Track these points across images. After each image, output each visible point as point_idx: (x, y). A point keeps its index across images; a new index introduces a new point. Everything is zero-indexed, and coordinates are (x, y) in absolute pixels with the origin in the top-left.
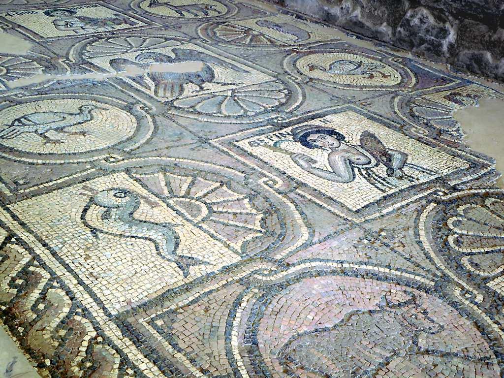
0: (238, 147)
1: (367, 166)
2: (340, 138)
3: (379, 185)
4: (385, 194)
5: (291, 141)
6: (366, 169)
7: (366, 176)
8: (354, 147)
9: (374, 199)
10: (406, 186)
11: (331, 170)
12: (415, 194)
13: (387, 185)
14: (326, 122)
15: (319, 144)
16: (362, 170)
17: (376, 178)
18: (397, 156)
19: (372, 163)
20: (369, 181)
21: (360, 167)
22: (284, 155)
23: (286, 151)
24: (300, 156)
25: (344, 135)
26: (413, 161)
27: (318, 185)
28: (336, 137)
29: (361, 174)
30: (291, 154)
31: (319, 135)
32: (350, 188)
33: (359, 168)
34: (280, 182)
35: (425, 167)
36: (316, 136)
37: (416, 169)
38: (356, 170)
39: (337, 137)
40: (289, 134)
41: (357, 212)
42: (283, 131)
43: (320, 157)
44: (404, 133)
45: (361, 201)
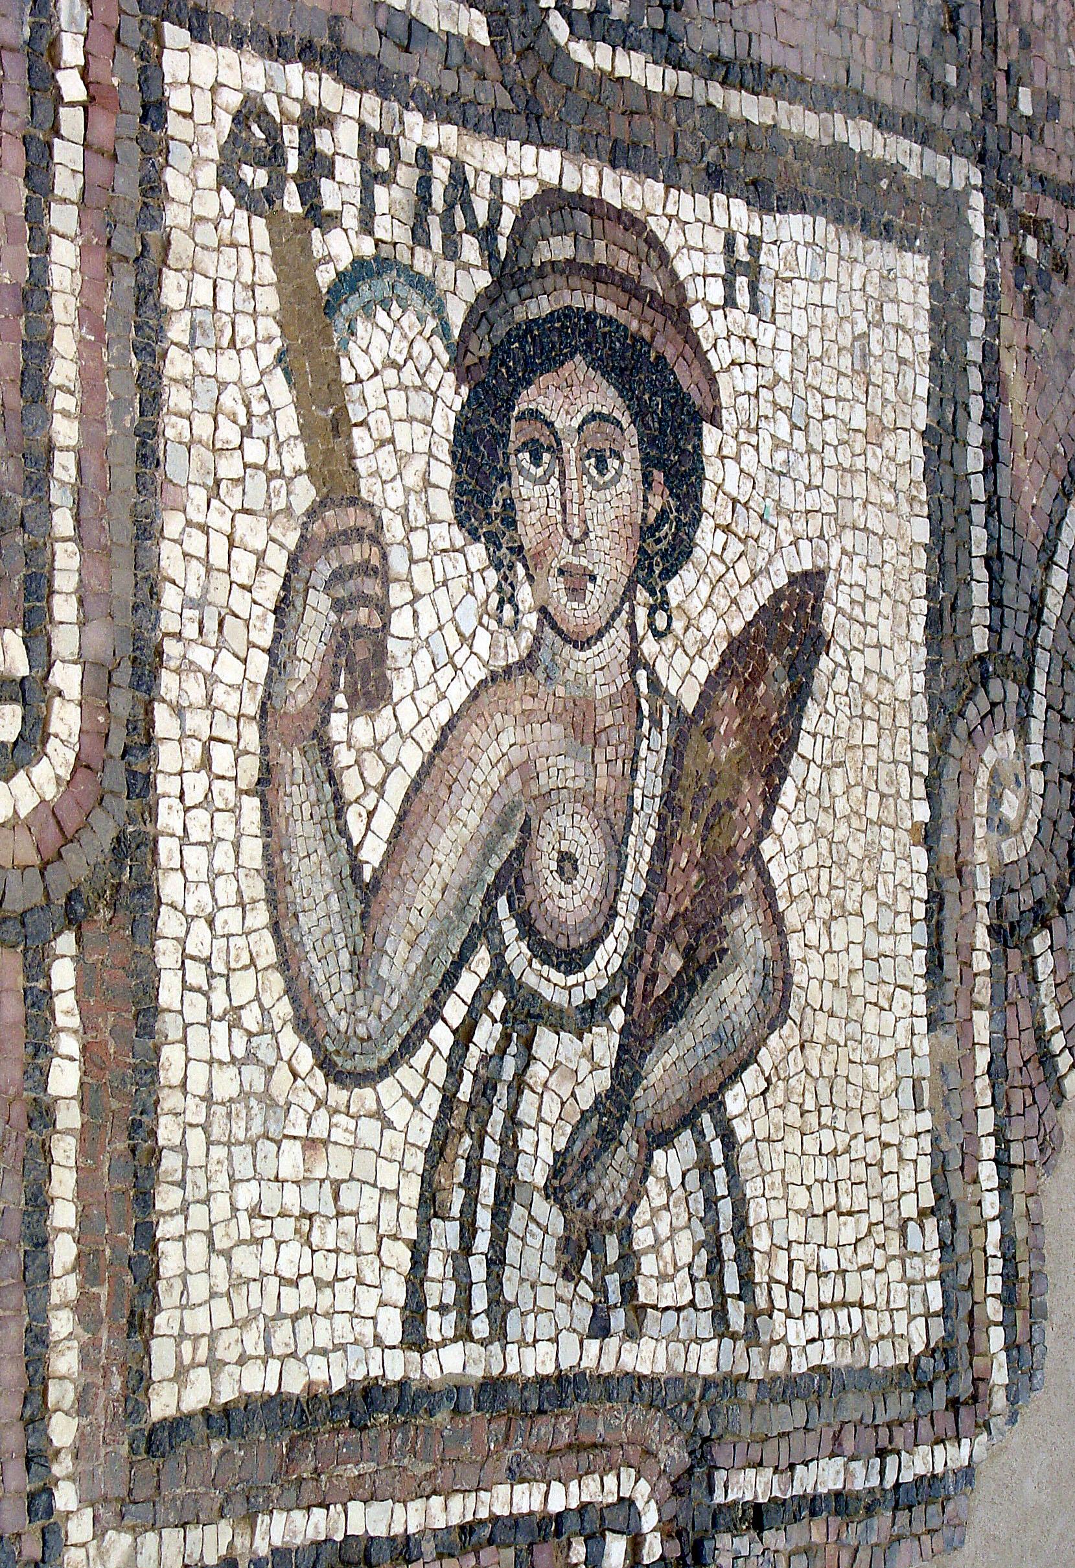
0: (154, 110)
1: (551, 985)
2: (661, 551)
3: (447, 1234)
4: (395, 1366)
5: (444, 329)
6: (527, 1016)
7: (465, 1092)
8: (641, 693)
9: (318, 1370)
10: (538, 1362)
11: (373, 853)
12: (516, 1476)
13: (478, 1269)
14: (742, 282)
15: (532, 493)
16: (498, 1003)
17: (491, 1151)
18: (735, 990)
19: (591, 970)
20: (437, 1153)
21: (517, 952)
22: (296, 457)
23: (340, 425)
24: (356, 553)
25: (707, 538)
26: (756, 1104)
27: (196, 975)
28: (657, 503)
29: (464, 1035)
30: (336, 480)
31: (605, 398)
32: (311, 1144)
33: (499, 976)
34: (59, 758)
35: (756, 1212)
36: (570, 398)
37: (711, 1202)
38: (467, 985)
39: (663, 515)
40: (487, 235)
41: (161, 1440)
42: (489, 157)
43: (445, 617)
44: (938, 754)
45: (253, 1341)
